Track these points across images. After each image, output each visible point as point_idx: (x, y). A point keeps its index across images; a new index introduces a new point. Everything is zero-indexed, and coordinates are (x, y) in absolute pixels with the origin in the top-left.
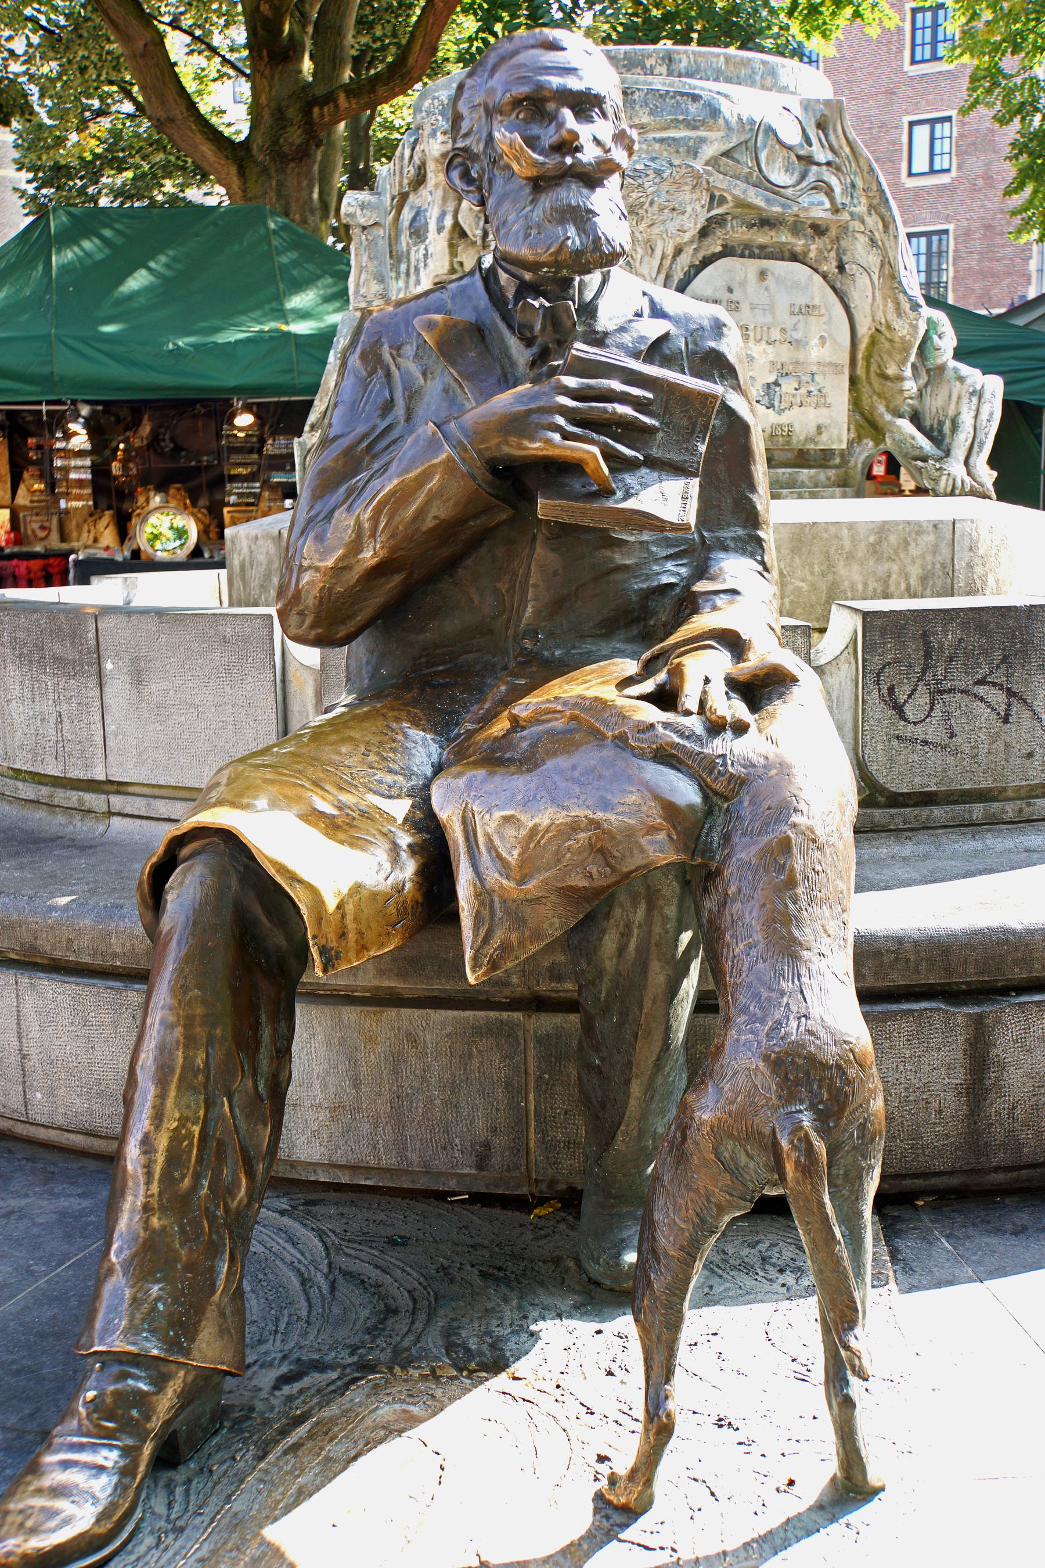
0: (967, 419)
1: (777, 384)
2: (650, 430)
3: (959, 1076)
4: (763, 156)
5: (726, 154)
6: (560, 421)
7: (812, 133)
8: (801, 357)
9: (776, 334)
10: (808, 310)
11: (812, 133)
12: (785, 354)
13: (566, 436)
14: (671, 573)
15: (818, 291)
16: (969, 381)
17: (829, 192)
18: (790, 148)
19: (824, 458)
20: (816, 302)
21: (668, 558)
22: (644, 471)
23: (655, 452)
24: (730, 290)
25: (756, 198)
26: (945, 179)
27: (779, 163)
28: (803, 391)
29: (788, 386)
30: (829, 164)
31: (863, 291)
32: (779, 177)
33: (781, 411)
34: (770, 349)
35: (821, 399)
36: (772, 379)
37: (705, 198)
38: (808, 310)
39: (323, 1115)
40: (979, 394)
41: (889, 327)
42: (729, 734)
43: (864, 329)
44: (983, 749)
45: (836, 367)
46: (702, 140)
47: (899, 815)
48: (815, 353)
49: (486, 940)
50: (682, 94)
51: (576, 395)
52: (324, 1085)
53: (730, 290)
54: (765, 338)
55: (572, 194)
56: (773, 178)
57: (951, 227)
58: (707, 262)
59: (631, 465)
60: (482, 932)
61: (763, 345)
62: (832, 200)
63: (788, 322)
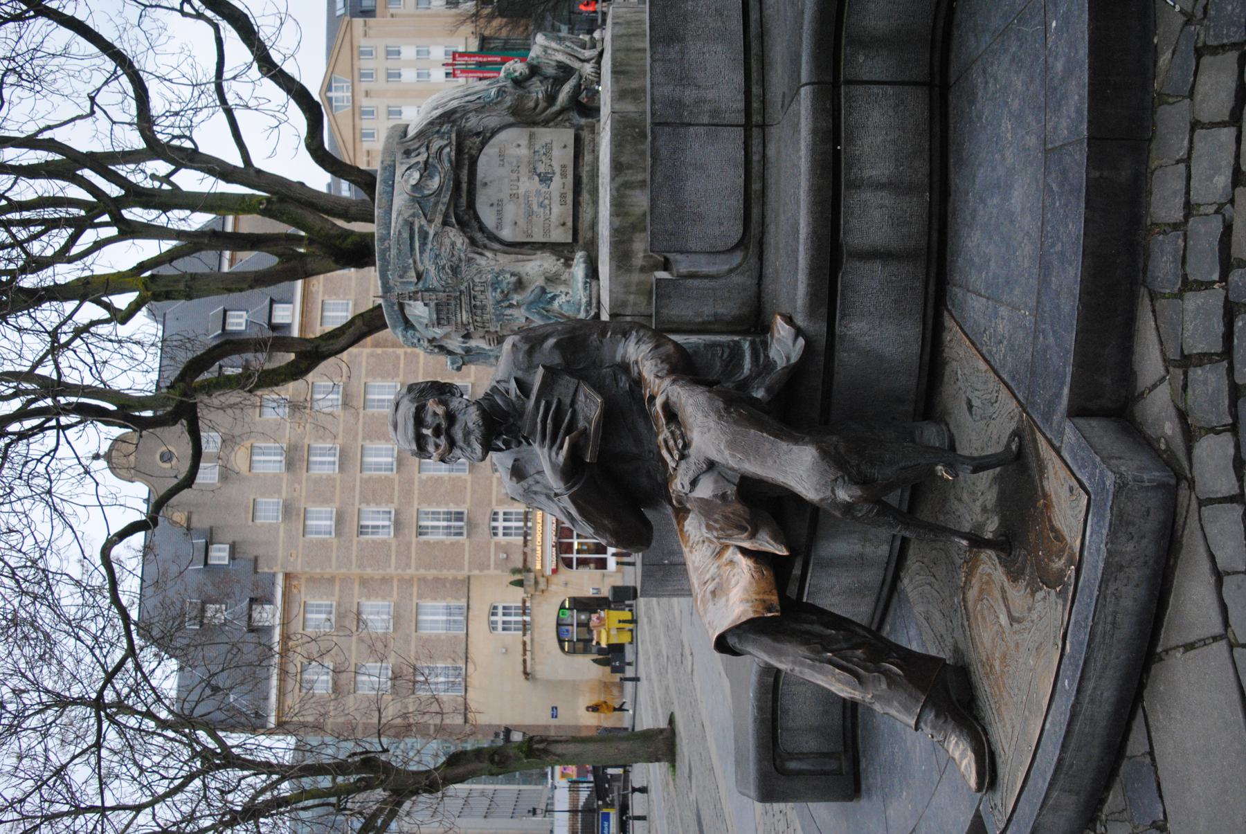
0: (560, 57)
1: (539, 175)
2: (559, 401)
3: (877, 266)
5: (425, 216)
6: (555, 448)
8: (526, 160)
9: (514, 176)
10: (501, 156)
12: (524, 170)
14: (624, 383)
15: (490, 151)
17: (441, 149)
18: (421, 176)
19: (578, 140)
20: (497, 150)
23: (568, 401)
24: (492, 205)
25: (446, 198)
27: (429, 183)
28: (544, 158)
29: (541, 168)
31: (491, 121)
32: (435, 183)
35: (548, 147)
36: (537, 178)
37: (448, 228)
38: (501, 156)
39: (868, 544)
40: (545, 49)
41: (509, 108)
43: (512, 120)
45: (532, 136)
47: (755, 230)
48: (524, 152)
53: (492, 205)
55: (458, 433)
56: (436, 186)
58: (477, 218)
61: (520, 184)
62: (446, 146)
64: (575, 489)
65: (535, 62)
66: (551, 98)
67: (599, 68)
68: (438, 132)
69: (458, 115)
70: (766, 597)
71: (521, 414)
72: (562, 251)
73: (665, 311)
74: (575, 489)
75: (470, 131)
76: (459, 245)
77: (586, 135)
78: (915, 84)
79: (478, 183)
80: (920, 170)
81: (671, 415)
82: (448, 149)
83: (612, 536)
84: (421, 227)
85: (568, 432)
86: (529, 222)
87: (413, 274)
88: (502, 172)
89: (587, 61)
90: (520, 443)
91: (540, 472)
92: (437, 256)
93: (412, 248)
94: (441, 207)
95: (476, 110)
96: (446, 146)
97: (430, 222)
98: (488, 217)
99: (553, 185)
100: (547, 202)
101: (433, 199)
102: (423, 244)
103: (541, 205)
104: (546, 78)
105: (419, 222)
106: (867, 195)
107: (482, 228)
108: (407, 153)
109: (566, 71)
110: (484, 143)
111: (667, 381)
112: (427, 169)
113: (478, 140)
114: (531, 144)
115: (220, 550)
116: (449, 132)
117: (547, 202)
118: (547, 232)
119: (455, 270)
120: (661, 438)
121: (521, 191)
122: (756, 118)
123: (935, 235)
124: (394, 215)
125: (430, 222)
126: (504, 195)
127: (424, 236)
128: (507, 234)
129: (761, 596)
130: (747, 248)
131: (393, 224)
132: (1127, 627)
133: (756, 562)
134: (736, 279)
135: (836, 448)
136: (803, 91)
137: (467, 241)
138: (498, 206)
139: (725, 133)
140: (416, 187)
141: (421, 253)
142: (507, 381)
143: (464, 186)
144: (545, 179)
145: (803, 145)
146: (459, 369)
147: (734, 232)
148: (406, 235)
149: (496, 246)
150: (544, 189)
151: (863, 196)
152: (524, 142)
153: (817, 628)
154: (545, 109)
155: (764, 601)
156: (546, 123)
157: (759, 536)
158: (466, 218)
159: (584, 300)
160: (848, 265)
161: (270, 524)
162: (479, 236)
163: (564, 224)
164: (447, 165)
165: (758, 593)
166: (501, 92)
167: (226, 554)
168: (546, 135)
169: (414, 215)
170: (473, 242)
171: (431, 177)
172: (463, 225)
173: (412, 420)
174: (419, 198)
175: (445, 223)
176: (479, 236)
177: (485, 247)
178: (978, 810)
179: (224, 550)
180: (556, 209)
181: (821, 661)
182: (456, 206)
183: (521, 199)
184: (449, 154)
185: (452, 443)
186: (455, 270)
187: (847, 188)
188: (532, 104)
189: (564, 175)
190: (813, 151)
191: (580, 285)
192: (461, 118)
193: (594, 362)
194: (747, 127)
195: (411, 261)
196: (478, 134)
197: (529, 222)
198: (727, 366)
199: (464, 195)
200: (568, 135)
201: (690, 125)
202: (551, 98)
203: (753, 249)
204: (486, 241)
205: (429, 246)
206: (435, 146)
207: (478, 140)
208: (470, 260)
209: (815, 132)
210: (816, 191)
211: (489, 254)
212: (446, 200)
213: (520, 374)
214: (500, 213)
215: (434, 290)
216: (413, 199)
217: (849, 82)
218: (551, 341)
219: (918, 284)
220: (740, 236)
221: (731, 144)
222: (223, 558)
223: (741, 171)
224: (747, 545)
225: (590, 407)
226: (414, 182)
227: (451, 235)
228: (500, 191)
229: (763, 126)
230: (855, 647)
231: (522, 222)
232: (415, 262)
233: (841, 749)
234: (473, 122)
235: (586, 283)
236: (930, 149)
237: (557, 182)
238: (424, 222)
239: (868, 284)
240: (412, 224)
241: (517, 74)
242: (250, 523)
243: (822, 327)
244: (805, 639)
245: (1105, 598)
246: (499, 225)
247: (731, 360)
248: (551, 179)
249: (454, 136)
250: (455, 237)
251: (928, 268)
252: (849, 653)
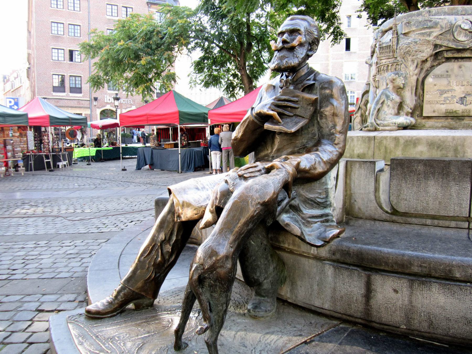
1: (465, 97)
3: (363, 291)
4: (455, 34)
5: (441, 35)
9: (465, 83)
18: (466, 30)
22: (294, 118)
27: (462, 35)
32: (462, 38)
33: (466, 105)
34: (463, 88)
36: (463, 96)
37: (432, 47)
44: (431, 203)
46: (432, 32)
50: (426, 21)
53: (447, 72)
54: (460, 84)
56: (459, 39)
58: (439, 64)
61: (460, 86)
72: (417, 110)
73: (357, 165)
76: (422, 54)
87: (406, 31)
92: (416, 42)
99: (458, 105)
105: (436, 32)
107: (432, 67)
111: (290, 169)
117: (448, 102)
118: (430, 102)
128: (429, 80)
130: (392, 214)
131: (436, 17)
135: (221, 267)
137: (424, 59)
138: (447, 75)
142: (315, 80)
145: (442, 256)
146: (366, 63)
147: (402, 208)
148: (429, 24)
149: (422, 75)
159: (386, 123)
160: (363, 273)
162: (428, 65)
169: (442, 27)
171: (466, 36)
172: (436, 56)
173: (292, 28)
174: (451, 30)
175: (436, 46)
176: (428, 65)
187: (412, 280)
190: (439, 263)
191: (394, 121)
198: (312, 200)
205: (422, 38)
211: (417, 71)
215: (398, 43)
226: (462, 26)
235: (395, 124)
247: (315, 203)
248: (462, 103)
250: (428, 51)
251: (360, 318)
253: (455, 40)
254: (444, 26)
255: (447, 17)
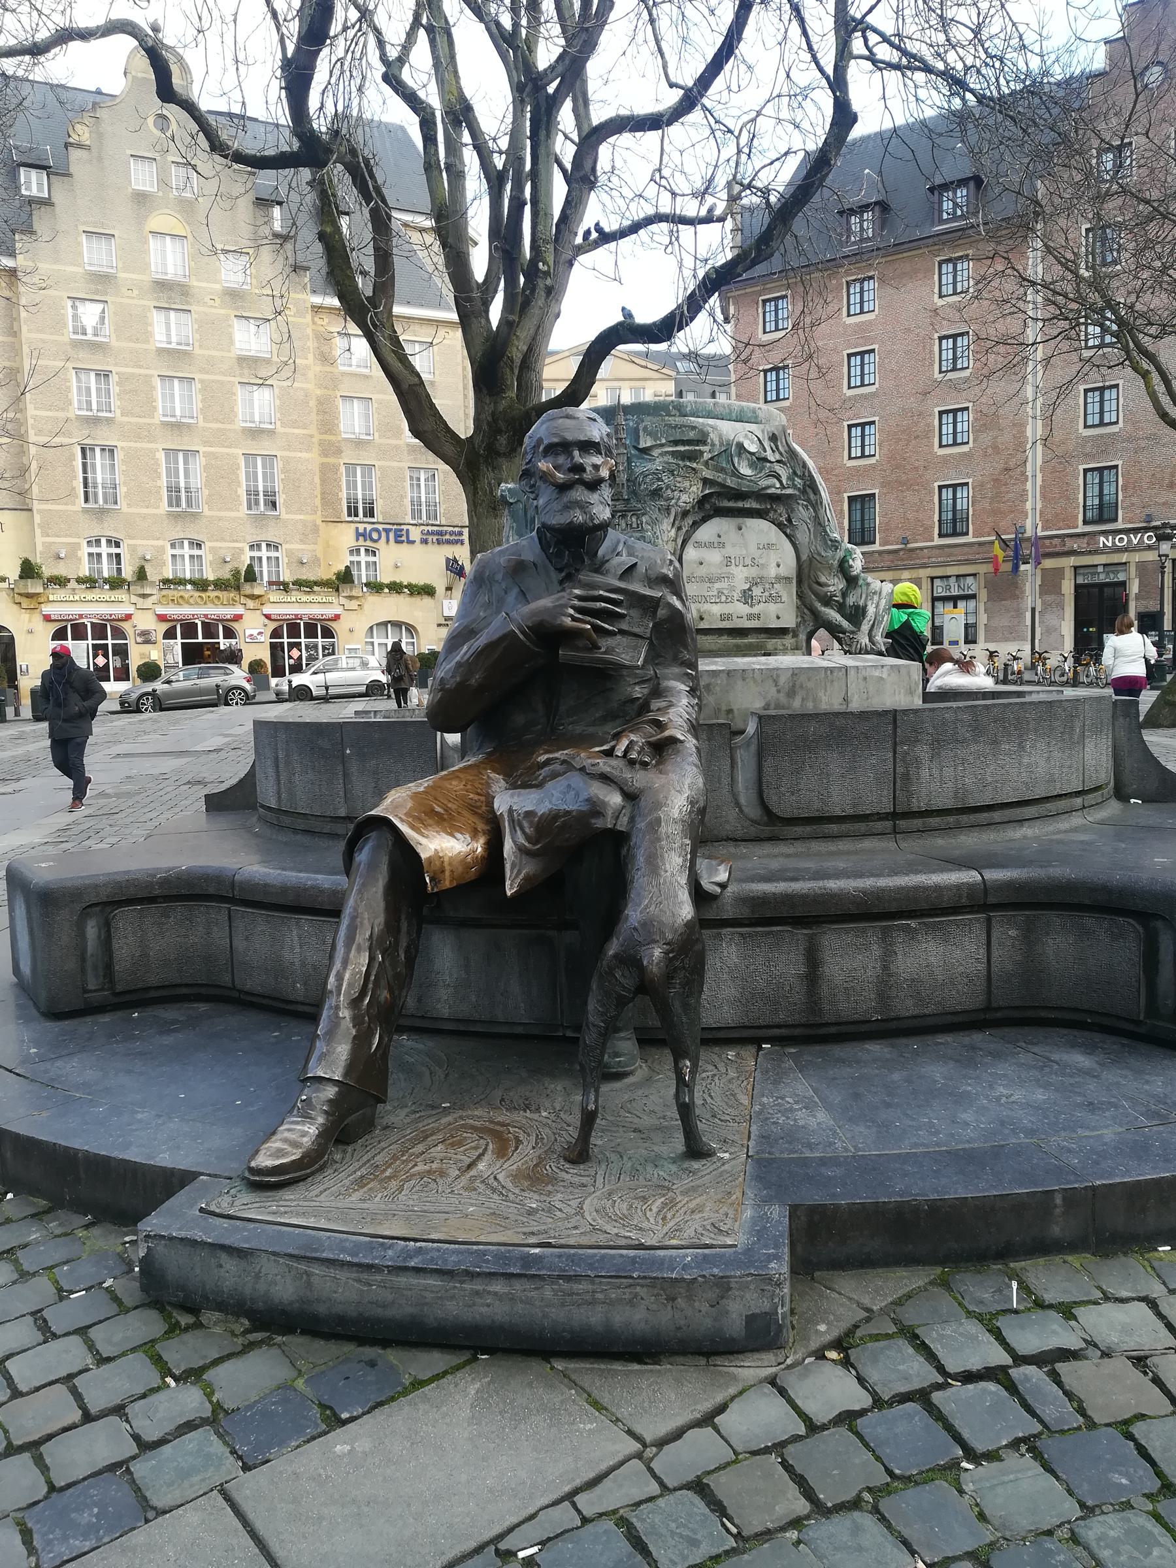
0: (871, 610)
1: (750, 589)
2: (622, 616)
3: (802, 970)
5: (711, 459)
6: (571, 611)
7: (766, 444)
10: (769, 546)
11: (766, 444)
12: (753, 572)
13: (574, 619)
16: (872, 586)
19: (782, 632)
21: (637, 683)
22: (619, 637)
24: (719, 536)
26: (965, 448)
27: (745, 463)
28: (767, 594)
29: (757, 591)
30: (778, 461)
31: (803, 536)
32: (745, 470)
36: (747, 586)
37: (700, 485)
38: (769, 546)
41: (819, 554)
42: (637, 766)
43: (804, 557)
45: (788, 579)
48: (772, 572)
49: (517, 876)
51: (581, 598)
52: (451, 975)
53: (719, 536)
55: (579, 494)
57: (970, 481)
58: (704, 520)
59: (611, 634)
60: (515, 871)
61: (741, 567)
62: (781, 482)
63: (757, 554)
64: (521, 637)
65: (861, 582)
66: (827, 601)
67: (867, 653)
68: (795, 473)
69: (812, 496)
70: (447, 873)
71: (599, 568)
74: (521, 637)
75: (793, 510)
77: (789, 641)
78: (989, 992)
79: (740, 520)
80: (905, 1006)
81: (663, 748)
82: (778, 485)
83: (458, 684)
84: (702, 453)
85: (594, 626)
86: (702, 580)
87: (649, 444)
88: (753, 550)
89: (871, 640)
90: (560, 570)
91: (524, 596)
93: (676, 443)
94: (720, 477)
95: (817, 517)
96: (781, 482)
97: (706, 464)
98: (708, 531)
100: (723, 599)
101: (729, 467)
102: (684, 456)
103: (720, 592)
104: (844, 594)
106: (876, 950)
107: (696, 525)
108: (773, 438)
109: (856, 615)
110: (780, 526)
112: (759, 461)
113: (783, 519)
114: (779, 579)
115: (40, 185)
116: (794, 487)
119: (656, 494)
120: (633, 737)
121: (733, 569)
122: (902, 824)
123: (833, 1030)
124: (711, 421)
125: (706, 464)
126: (729, 551)
127: (694, 456)
129: (447, 868)
132: (594, 1318)
133: (483, 857)
134: (732, 814)
136: (975, 873)
139: (887, 792)
140: (740, 446)
141: (673, 453)
143: (740, 504)
144: (747, 597)
148: (692, 435)
149: (680, 542)
150: (737, 595)
151: (875, 947)
152: (783, 571)
153: (404, 943)
154: (816, 594)
155: (443, 872)
156: (800, 596)
157: (525, 858)
158: (707, 506)
161: (81, 254)
162: (689, 521)
163: (702, 619)
164: (763, 483)
165: (450, 864)
166: (835, 545)
167: (34, 192)
168: (788, 595)
169: (713, 445)
170: (685, 514)
171: (752, 465)
172: (702, 501)
175: (706, 482)
176: (689, 521)
177: (679, 528)
178: (194, 1175)
179: (40, 189)
180: (716, 609)
181: (370, 948)
182: (719, 494)
183: (725, 569)
184: (774, 486)
185: (563, 488)
186: (656, 494)
188: (823, 579)
189: (750, 617)
192: (808, 500)
193: (659, 656)
194: (894, 816)
195: (664, 441)
196: (789, 520)
197: (702, 580)
199: (731, 504)
200: (789, 620)
201: (895, 753)
202: (827, 601)
203: (767, 830)
204: (684, 530)
206: (784, 473)
207: (783, 519)
208: (668, 510)
209: (938, 888)
210: (879, 895)
212: (729, 482)
213: (641, 569)
214: (710, 545)
216: (729, 444)
217: (989, 920)
218: (678, 604)
219: (782, 1017)
220: (780, 814)
221: (878, 799)
222: (28, 188)
223: (851, 812)
224: (508, 847)
225: (627, 653)
227: (694, 489)
228: (734, 546)
229: (895, 831)
230: (391, 991)
231: (702, 571)
232: (662, 445)
233: (119, 988)
234: (802, 513)
236: (925, 1016)
237: (744, 609)
238: (706, 456)
239: (783, 962)
240: (704, 443)
241: (851, 562)
242: (82, 228)
243: (728, 913)
244: (392, 925)
245: (630, 1286)
246: (698, 545)
249: (789, 491)
252: (383, 982)
253: (736, 473)
254: (717, 443)
255: (718, 423)
